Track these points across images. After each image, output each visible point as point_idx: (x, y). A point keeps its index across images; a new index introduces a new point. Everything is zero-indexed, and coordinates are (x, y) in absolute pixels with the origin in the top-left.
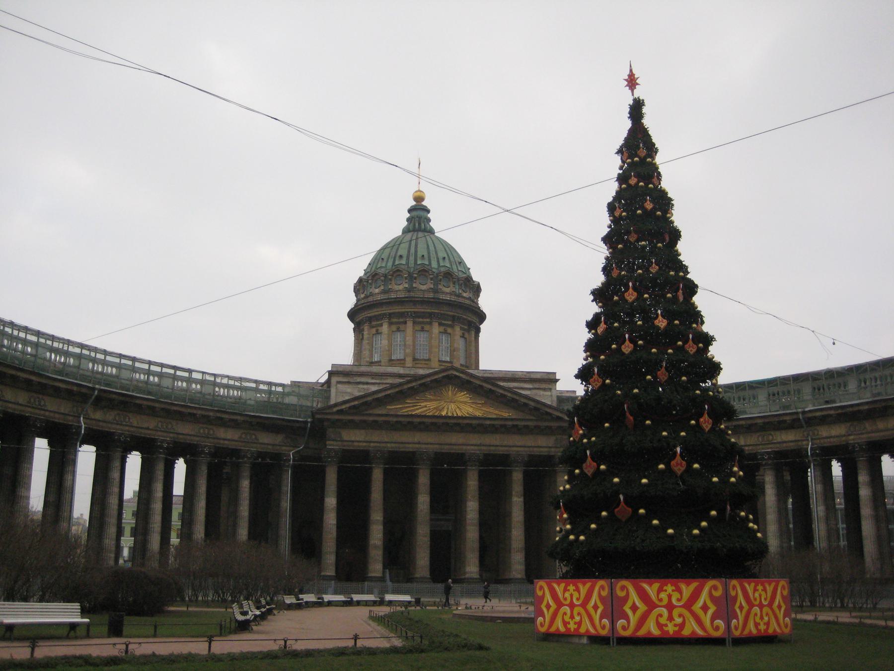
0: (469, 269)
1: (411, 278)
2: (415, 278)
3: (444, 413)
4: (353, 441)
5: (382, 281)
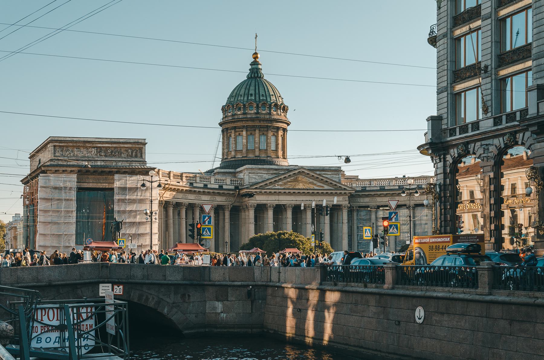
0: (283, 99)
1: (258, 107)
2: (260, 107)
3: (297, 187)
4: (260, 200)
5: (242, 108)
